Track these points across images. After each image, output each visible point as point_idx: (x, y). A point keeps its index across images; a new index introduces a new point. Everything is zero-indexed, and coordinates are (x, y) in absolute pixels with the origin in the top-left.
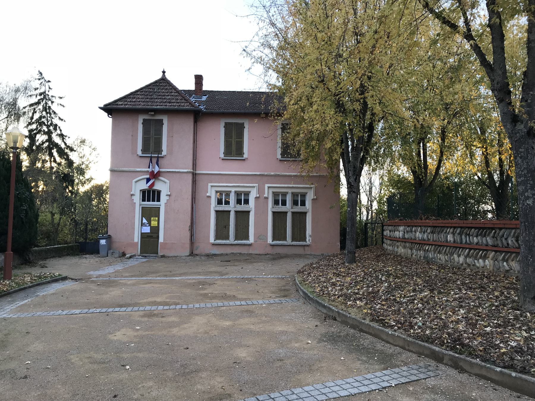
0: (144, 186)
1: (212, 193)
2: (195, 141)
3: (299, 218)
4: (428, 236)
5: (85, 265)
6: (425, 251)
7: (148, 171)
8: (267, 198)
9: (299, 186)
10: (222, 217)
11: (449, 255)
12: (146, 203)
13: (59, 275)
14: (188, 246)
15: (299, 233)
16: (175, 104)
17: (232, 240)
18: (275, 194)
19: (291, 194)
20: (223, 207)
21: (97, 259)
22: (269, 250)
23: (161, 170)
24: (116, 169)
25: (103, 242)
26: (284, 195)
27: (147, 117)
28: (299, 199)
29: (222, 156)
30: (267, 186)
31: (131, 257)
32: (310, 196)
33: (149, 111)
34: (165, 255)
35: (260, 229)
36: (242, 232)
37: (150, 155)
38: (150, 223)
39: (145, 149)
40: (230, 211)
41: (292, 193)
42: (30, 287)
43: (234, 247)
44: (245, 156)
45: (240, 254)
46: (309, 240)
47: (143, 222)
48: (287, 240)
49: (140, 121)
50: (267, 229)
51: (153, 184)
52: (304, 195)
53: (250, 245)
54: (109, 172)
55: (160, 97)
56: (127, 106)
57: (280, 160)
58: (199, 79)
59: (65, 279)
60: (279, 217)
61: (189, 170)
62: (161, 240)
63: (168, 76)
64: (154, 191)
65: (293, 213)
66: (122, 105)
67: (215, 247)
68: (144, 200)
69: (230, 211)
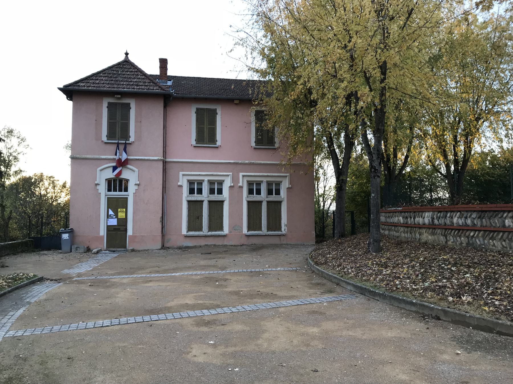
0: (110, 174)
1: (184, 182)
2: (165, 127)
3: (274, 208)
4: (473, 222)
5: (47, 262)
6: (468, 237)
7: (114, 159)
8: (241, 187)
9: (274, 174)
10: (195, 207)
11: (507, 241)
12: (112, 193)
13: (34, 275)
14: (160, 238)
15: (274, 223)
16: (143, 87)
17: (264, 230)
18: (250, 184)
19: (266, 183)
20: (196, 197)
21: (61, 256)
22: (244, 241)
23: (129, 157)
24: (78, 156)
25: (65, 236)
26: (259, 184)
27: (112, 100)
28: (273, 189)
29: (194, 143)
30: (241, 174)
31: (98, 252)
32: (285, 185)
33: (112, 95)
34: (135, 249)
35: (234, 219)
36: (216, 223)
37: (117, 142)
38: (116, 215)
39: (111, 135)
40: (202, 201)
41: (267, 182)
42: (9, 292)
43: (208, 238)
44: (218, 143)
45: (215, 245)
46: (285, 230)
47: (110, 213)
48: (263, 229)
49: (105, 105)
50: (242, 219)
51: (120, 173)
52: (278, 184)
53: (225, 236)
54: (70, 159)
55: (125, 80)
56: (90, 88)
57: (255, 148)
58: (163, 63)
59: (41, 280)
60: (254, 207)
61: (160, 158)
62: (130, 232)
63: (131, 58)
64: (121, 181)
65: (268, 202)
66: (84, 86)
67: (188, 239)
68: (109, 190)
69: (202, 201)
